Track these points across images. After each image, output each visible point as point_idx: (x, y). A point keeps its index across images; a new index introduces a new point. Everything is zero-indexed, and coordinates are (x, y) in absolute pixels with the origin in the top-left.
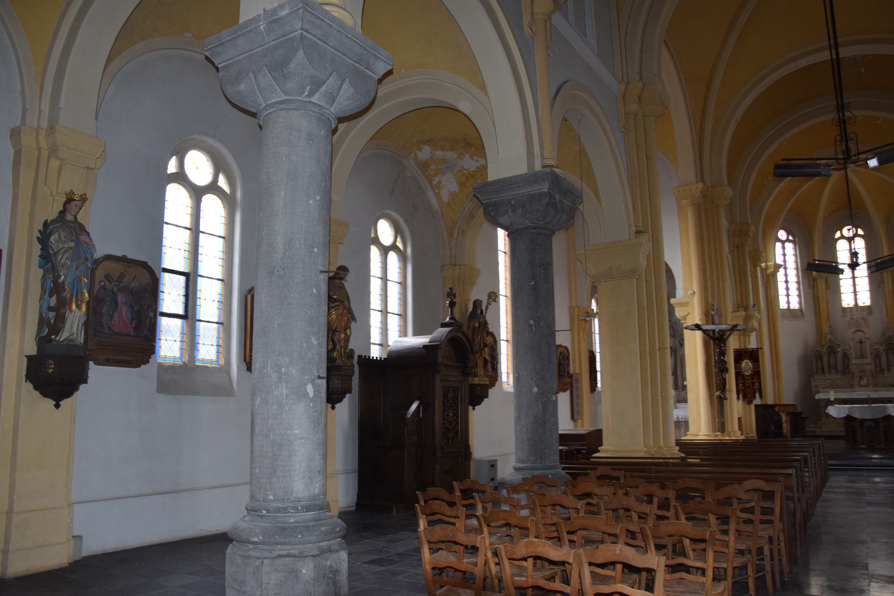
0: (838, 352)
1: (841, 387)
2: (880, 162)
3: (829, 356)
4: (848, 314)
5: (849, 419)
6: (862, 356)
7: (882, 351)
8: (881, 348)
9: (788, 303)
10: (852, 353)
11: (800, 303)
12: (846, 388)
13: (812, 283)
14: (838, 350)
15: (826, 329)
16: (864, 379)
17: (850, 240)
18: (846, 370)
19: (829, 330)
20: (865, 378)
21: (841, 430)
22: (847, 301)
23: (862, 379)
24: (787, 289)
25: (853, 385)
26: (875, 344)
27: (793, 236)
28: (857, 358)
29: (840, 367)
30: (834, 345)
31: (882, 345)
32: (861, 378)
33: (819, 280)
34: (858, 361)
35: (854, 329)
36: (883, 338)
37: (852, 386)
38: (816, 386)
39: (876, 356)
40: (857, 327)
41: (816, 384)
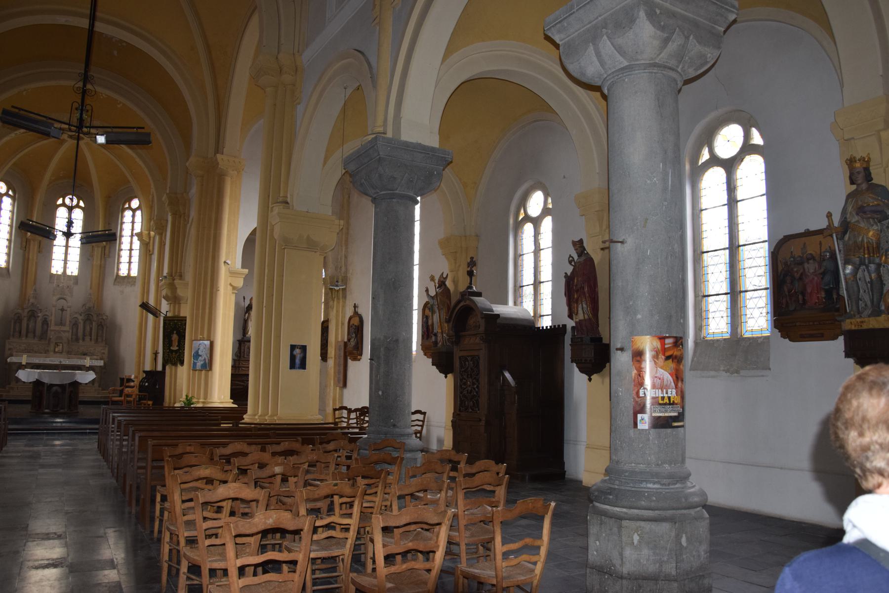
0: (38, 317)
1: (36, 352)
2: (108, 141)
3: (29, 320)
4: (55, 281)
5: (38, 383)
6: (62, 323)
7: (80, 321)
8: (80, 318)
10: (52, 319)
11: (8, 262)
13: (24, 244)
14: (39, 315)
15: (30, 292)
16: (60, 345)
17: (70, 209)
18: (44, 336)
19: (33, 294)
20: (61, 344)
21: (28, 394)
22: (57, 267)
23: (58, 345)
25: (48, 351)
26: (76, 313)
27: (14, 191)
28: (56, 325)
31: (81, 315)
32: (57, 344)
33: (32, 242)
34: (57, 328)
35: (58, 296)
36: (84, 308)
37: (46, 352)
38: (10, 349)
39: (75, 325)
41: (12, 347)
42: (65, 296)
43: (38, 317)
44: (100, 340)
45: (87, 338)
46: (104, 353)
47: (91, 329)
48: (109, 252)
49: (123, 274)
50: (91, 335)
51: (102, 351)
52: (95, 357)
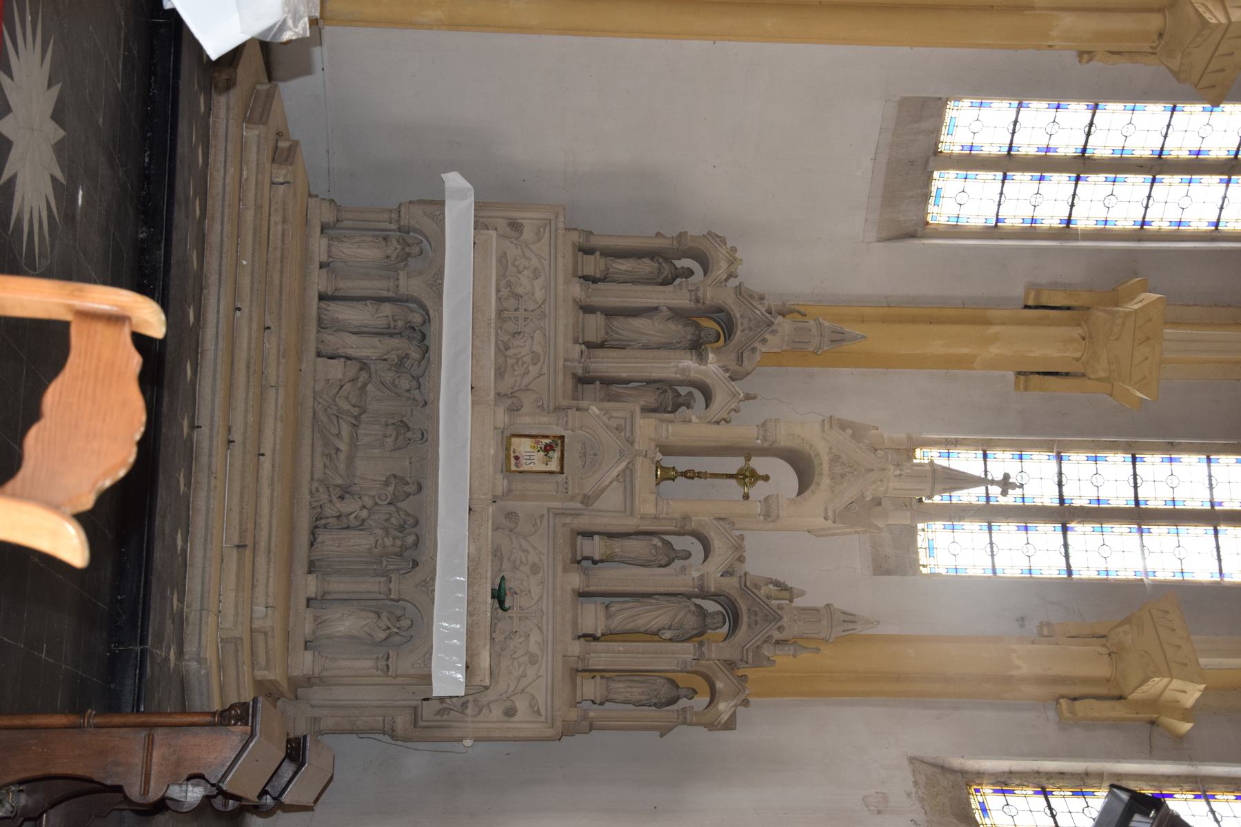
0: (702, 358)
1: (503, 349)
3: (677, 314)
8: (714, 568)
9: (971, 162)
11: (955, 231)
12: (500, 373)
20: (554, 466)
23: (548, 449)
24: (1044, 164)
29: (608, 364)
30: (738, 336)
32: (553, 445)
33: (1076, 332)
40: (835, 459)
41: (528, 234)
42: (826, 482)
43: (702, 358)
44: (590, 688)
45: (592, 618)
46: (510, 712)
47: (654, 635)
48: (1091, 724)
49: (984, 810)
50: (610, 636)
51: (521, 705)
52: (485, 660)
